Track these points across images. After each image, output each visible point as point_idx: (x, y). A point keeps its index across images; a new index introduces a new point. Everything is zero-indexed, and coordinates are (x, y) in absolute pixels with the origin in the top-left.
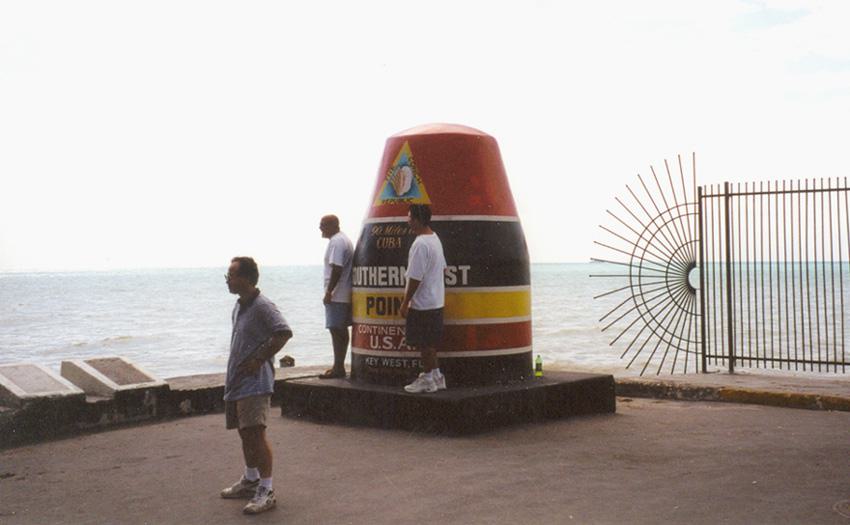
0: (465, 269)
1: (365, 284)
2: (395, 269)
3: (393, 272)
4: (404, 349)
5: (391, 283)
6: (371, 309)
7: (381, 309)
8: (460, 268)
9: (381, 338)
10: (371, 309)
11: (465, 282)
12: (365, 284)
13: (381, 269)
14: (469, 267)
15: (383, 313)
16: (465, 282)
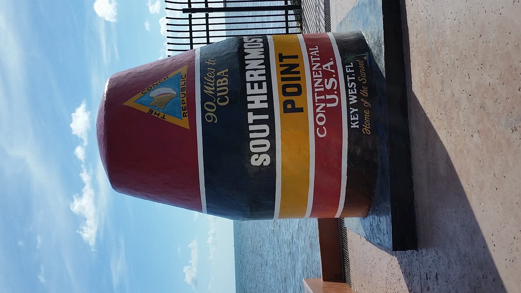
1: (266, 117)
2: (248, 74)
3: (252, 76)
4: (334, 67)
5: (264, 78)
7: (295, 90)
9: (327, 92)
12: (266, 117)
13: (249, 91)
15: (299, 86)
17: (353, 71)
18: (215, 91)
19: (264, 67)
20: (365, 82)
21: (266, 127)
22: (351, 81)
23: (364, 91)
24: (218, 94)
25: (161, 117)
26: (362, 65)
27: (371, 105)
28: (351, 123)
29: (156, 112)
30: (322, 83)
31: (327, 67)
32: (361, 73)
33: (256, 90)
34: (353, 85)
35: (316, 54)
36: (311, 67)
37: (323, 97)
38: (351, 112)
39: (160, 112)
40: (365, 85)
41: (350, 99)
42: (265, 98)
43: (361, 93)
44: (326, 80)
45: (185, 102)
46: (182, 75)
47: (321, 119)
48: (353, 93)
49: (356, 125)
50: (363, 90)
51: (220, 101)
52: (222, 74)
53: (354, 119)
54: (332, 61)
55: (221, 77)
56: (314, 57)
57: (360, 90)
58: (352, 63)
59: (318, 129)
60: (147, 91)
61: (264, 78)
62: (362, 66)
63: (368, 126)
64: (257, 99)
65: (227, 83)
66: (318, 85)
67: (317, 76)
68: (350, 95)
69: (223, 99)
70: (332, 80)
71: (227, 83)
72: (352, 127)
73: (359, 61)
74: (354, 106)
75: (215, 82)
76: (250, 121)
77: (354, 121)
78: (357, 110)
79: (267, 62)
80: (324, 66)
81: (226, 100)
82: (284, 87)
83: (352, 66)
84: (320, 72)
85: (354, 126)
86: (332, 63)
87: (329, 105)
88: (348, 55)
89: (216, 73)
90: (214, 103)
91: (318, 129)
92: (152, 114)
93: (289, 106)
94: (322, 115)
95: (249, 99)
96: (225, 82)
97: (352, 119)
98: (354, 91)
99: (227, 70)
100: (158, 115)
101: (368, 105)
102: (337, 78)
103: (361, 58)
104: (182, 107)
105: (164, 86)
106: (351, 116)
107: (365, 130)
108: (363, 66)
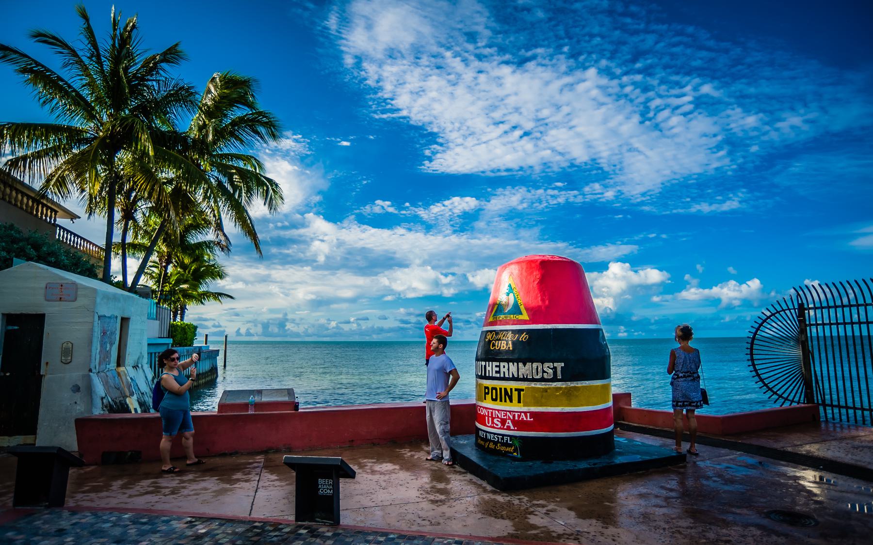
0: (559, 365)
2: (506, 364)
3: (504, 367)
4: (509, 428)
5: (502, 375)
8: (556, 364)
9: (493, 419)
11: (559, 377)
13: (495, 364)
14: (563, 364)
15: (495, 400)
16: (559, 377)
19: (511, 376)
22: (498, 438)
30: (498, 417)
31: (508, 423)
36: (510, 412)
37: (490, 415)
40: (495, 447)
42: (491, 375)
54: (514, 427)
55: (507, 344)
56: (519, 416)
61: (502, 375)
64: (490, 369)
65: (502, 348)
67: (503, 415)
69: (494, 345)
70: (500, 425)
74: (486, 435)
75: (505, 340)
79: (514, 379)
80: (510, 421)
82: (496, 389)
84: (505, 417)
86: (512, 428)
88: (520, 442)
93: (487, 391)
95: (490, 363)
103: (515, 451)
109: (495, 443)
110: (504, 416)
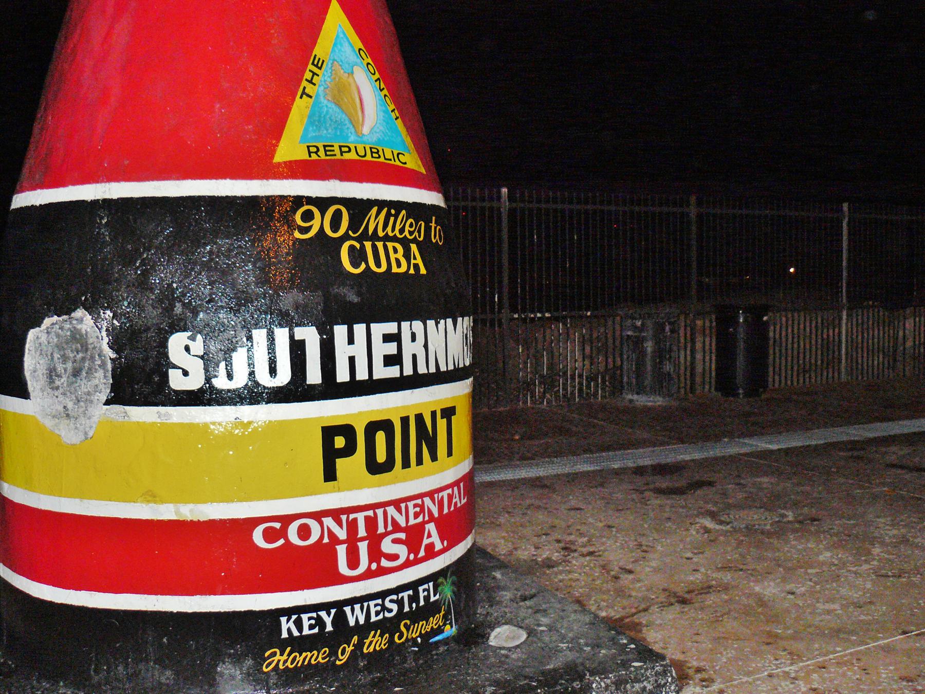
2: (418, 325)
4: (431, 553)
6: (340, 462)
7: (381, 456)
10: (340, 462)
12: (314, 376)
13: (379, 329)
15: (388, 466)
17: (422, 603)
18: (375, 237)
19: (433, 370)
20: (399, 639)
21: (284, 376)
23: (378, 640)
24: (368, 245)
25: (304, 88)
26: (435, 622)
27: (342, 664)
28: (294, 617)
29: (318, 75)
30: (397, 528)
32: (418, 626)
33: (382, 349)
34: (390, 611)
35: (454, 501)
37: (362, 532)
38: (323, 614)
39: (317, 85)
40: (391, 641)
41: (357, 607)
43: (373, 633)
44: (402, 536)
45: (347, 156)
46: (404, 155)
47: (304, 532)
48: (373, 611)
49: (289, 630)
50: (380, 638)
51: (352, 248)
52: (415, 258)
53: (306, 624)
55: (407, 255)
57: (379, 631)
58: (437, 597)
59: (277, 525)
60: (365, 63)
61: (408, 371)
62: (432, 623)
63: (286, 661)
65: (395, 269)
66: (392, 518)
67: (412, 512)
68: (368, 606)
70: (402, 551)
71: (395, 269)
72: (283, 620)
73: (443, 612)
74: (340, 619)
75: (394, 239)
76: (301, 333)
77: (299, 624)
78: (329, 628)
81: (355, 265)
82: (386, 426)
83: (433, 599)
84: (420, 519)
85: (287, 626)
87: (342, 550)
89: (415, 241)
90: (347, 232)
91: (277, 525)
92: (313, 64)
93: (340, 442)
94: (313, 539)
95: (360, 329)
96: (399, 265)
97: (305, 617)
98: (377, 613)
99: (423, 271)
100: (311, 82)
101: (342, 655)
102: (408, 564)
104: (333, 146)
105: (379, 106)
106: (314, 615)
107: (274, 654)
108: (432, 627)
109: (388, 626)
110: (416, 515)
